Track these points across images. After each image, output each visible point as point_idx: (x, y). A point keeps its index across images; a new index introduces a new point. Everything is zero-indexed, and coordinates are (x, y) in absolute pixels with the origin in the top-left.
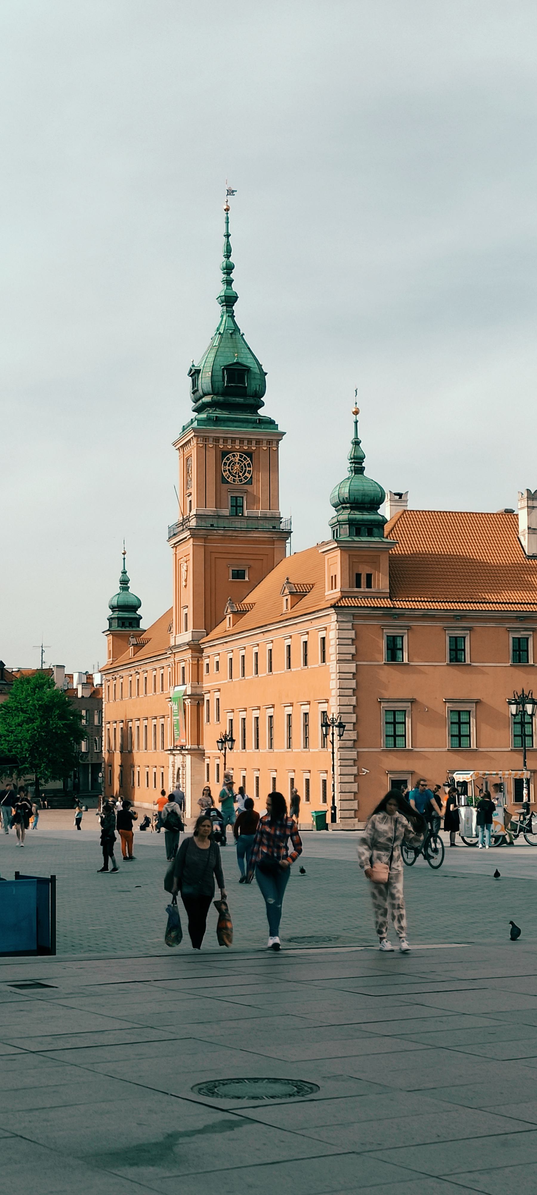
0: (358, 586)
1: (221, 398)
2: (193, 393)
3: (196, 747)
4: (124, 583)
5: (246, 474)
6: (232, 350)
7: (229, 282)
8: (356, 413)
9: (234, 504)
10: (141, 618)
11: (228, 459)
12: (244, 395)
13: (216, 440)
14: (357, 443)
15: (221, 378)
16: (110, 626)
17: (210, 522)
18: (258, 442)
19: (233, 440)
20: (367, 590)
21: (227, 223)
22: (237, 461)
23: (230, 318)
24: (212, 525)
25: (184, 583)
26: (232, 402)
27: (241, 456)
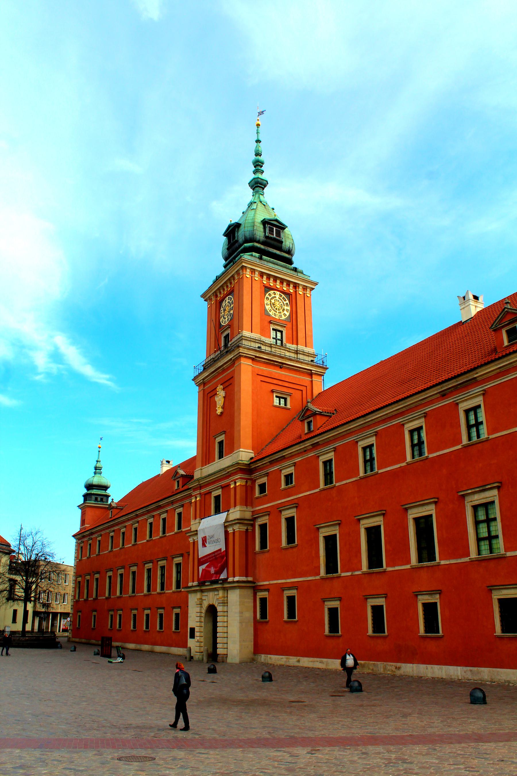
1: (262, 247)
2: (228, 249)
3: (244, 579)
4: (97, 470)
5: (285, 312)
9: (275, 337)
10: (110, 496)
11: (270, 295)
12: (280, 249)
13: (262, 274)
16: (85, 500)
17: (258, 345)
18: (296, 285)
19: (276, 279)
22: (277, 298)
23: (261, 196)
24: (259, 347)
25: (219, 411)
27: (281, 296)
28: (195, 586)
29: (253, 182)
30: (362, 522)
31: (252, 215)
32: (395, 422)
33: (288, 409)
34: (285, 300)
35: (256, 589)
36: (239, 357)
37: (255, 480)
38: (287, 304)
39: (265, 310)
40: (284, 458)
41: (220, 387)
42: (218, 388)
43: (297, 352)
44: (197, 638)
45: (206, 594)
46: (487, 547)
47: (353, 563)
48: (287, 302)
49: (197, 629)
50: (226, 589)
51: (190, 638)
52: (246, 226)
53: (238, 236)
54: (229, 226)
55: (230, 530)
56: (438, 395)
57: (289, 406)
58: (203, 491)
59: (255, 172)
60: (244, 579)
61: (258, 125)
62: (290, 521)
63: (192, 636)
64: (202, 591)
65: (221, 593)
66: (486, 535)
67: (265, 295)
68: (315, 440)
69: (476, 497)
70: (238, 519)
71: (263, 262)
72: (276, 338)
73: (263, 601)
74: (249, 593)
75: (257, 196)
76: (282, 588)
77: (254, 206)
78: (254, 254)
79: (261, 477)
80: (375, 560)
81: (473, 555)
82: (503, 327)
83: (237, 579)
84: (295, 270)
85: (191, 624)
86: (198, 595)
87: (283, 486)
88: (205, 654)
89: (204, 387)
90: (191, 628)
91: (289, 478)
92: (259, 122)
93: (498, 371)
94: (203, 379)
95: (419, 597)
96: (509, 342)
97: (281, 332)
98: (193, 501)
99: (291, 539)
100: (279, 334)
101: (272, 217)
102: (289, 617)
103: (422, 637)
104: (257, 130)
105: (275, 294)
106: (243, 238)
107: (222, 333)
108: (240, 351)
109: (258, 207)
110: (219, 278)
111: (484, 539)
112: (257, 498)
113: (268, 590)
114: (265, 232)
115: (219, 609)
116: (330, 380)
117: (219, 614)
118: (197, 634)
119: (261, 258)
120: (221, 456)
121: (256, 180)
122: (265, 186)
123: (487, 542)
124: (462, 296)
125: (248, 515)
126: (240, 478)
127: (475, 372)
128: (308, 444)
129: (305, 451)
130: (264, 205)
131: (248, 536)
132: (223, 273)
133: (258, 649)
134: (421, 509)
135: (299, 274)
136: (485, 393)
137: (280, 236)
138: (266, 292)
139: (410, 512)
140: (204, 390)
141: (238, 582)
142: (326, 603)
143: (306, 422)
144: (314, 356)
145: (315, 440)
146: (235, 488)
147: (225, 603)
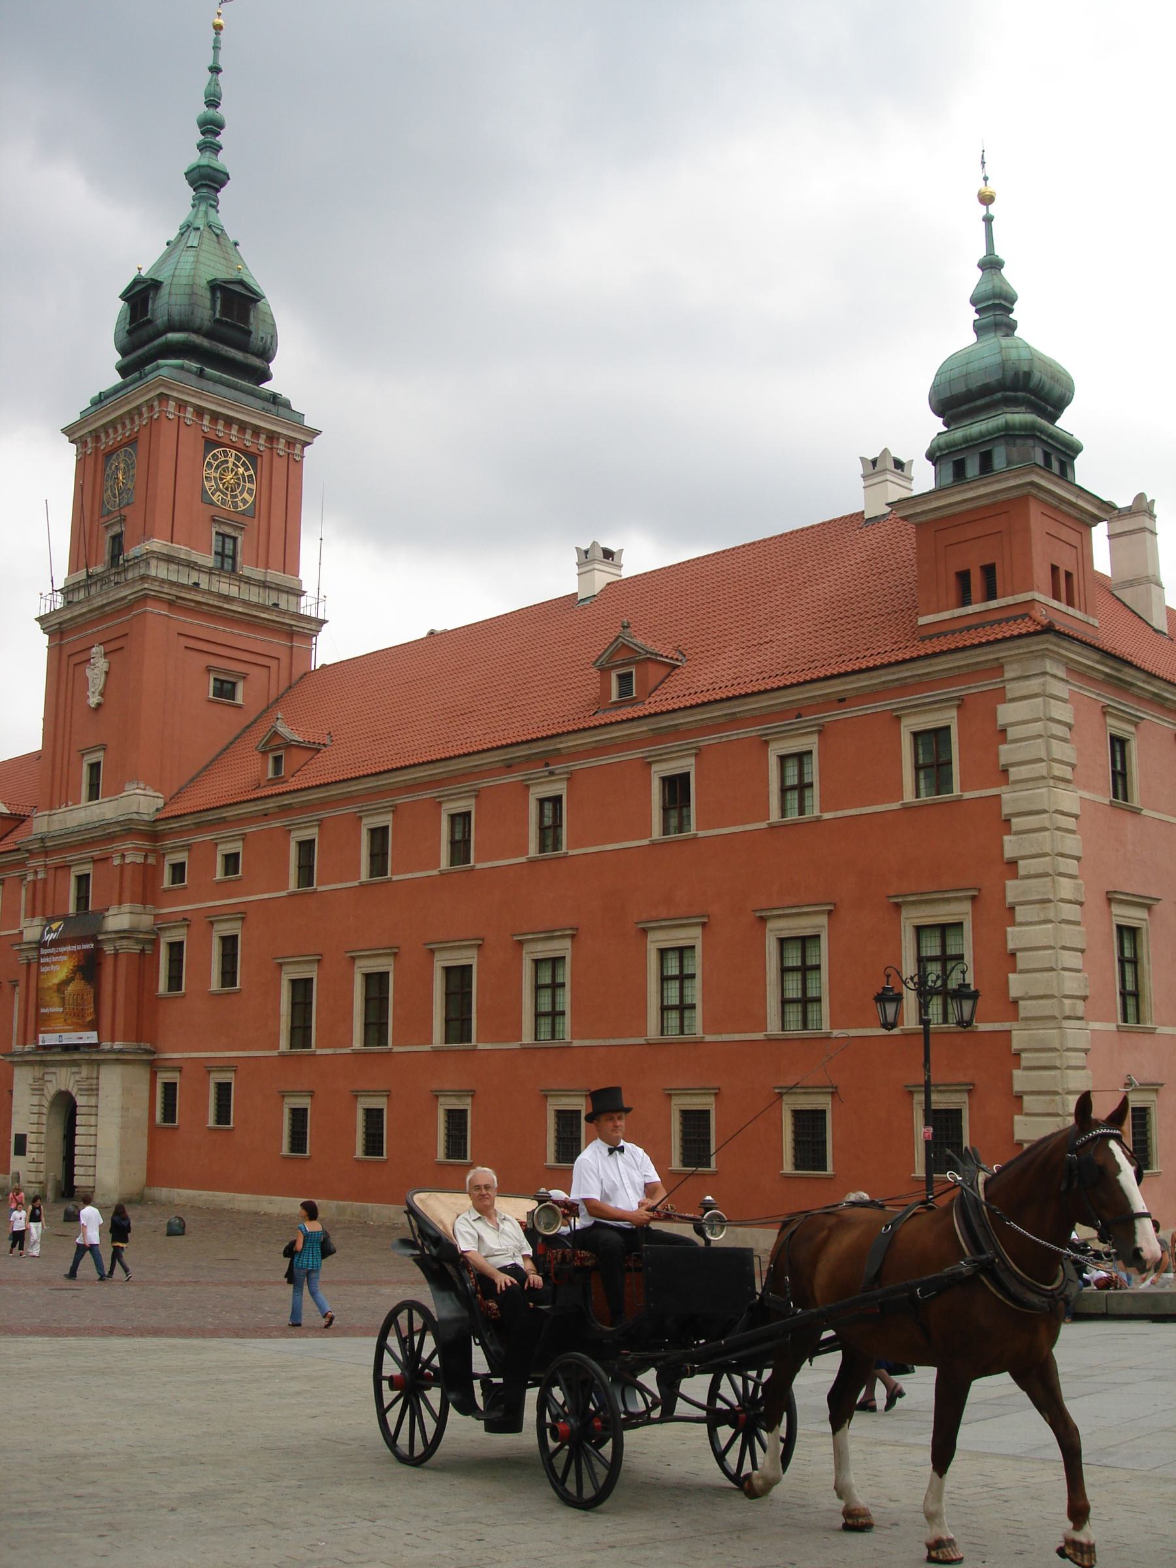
0: (1056, 596)
1: (206, 343)
2: (129, 332)
6: (222, 261)
7: (217, 149)
8: (986, 199)
9: (220, 550)
12: (244, 348)
13: (200, 412)
14: (991, 265)
15: (208, 304)
18: (272, 437)
19: (229, 421)
20: (1070, 610)
21: (216, 48)
22: (230, 465)
23: (212, 211)
25: (93, 700)
26: (223, 352)
27: (238, 458)
28: (29, 1053)
29: (195, 174)
30: (358, 963)
31: (188, 266)
32: (428, 795)
33: (239, 707)
34: (247, 469)
35: (154, 1067)
36: (144, 598)
37: (164, 855)
38: (250, 476)
39: (204, 491)
40: (223, 822)
41: (97, 650)
42: (94, 650)
43: (264, 585)
44: (30, 1156)
45: (53, 1070)
46: (549, 1028)
47: (338, 1032)
48: (252, 472)
49: (31, 1138)
50: (99, 1063)
51: (16, 1154)
52: (173, 292)
53: (153, 310)
54: (136, 282)
55: (108, 949)
56: (500, 765)
57: (239, 700)
58: (50, 861)
59: (203, 147)
60: (134, 1045)
61: (218, 28)
62: (229, 942)
63: (21, 1150)
64: (43, 1063)
65: (85, 1071)
66: (548, 1008)
67: (205, 458)
68: (286, 800)
69: (540, 946)
70: (124, 931)
71: (205, 383)
72: (221, 554)
73: (170, 1088)
74: (143, 1074)
75: (203, 208)
76: (208, 1067)
77: (193, 239)
78: (186, 363)
79: (175, 849)
80: (376, 1029)
81: (527, 1039)
82: (613, 668)
83: (118, 1045)
84: (274, 399)
85: (19, 1125)
86: (38, 1072)
87: (219, 875)
88: (50, 1186)
89: (61, 640)
90: (17, 1135)
91: (231, 861)
92: (220, 21)
93: (594, 745)
94: (60, 623)
95: (441, 1100)
96: (621, 695)
97: (235, 539)
98: (30, 878)
99: (229, 976)
100: (229, 544)
101: (230, 275)
102: (218, 1122)
103: (441, 1164)
104: (216, 41)
105: (225, 454)
106: (166, 318)
107: (107, 527)
108: (146, 586)
109: (205, 241)
110: (106, 398)
111: (545, 1014)
112: (166, 891)
113: (180, 1070)
114: (213, 308)
115: (80, 1100)
116: (329, 649)
117: (79, 1110)
118: (29, 1147)
119: (201, 374)
120: (94, 794)
121: (202, 170)
122: (223, 184)
123: (548, 1020)
124: (584, 548)
125: (146, 921)
126: (135, 849)
127: (558, 740)
128: (271, 804)
129: (266, 815)
130: (217, 235)
131: (145, 960)
132: (116, 390)
133: (154, 1176)
134: (455, 954)
135: (282, 410)
136: (571, 778)
137: (245, 318)
138: (207, 450)
139: (438, 956)
140: (61, 646)
141: (121, 1051)
142: (287, 1100)
143: (271, 756)
144: (299, 593)
145: (286, 800)
146: (122, 866)
147: (94, 1091)
